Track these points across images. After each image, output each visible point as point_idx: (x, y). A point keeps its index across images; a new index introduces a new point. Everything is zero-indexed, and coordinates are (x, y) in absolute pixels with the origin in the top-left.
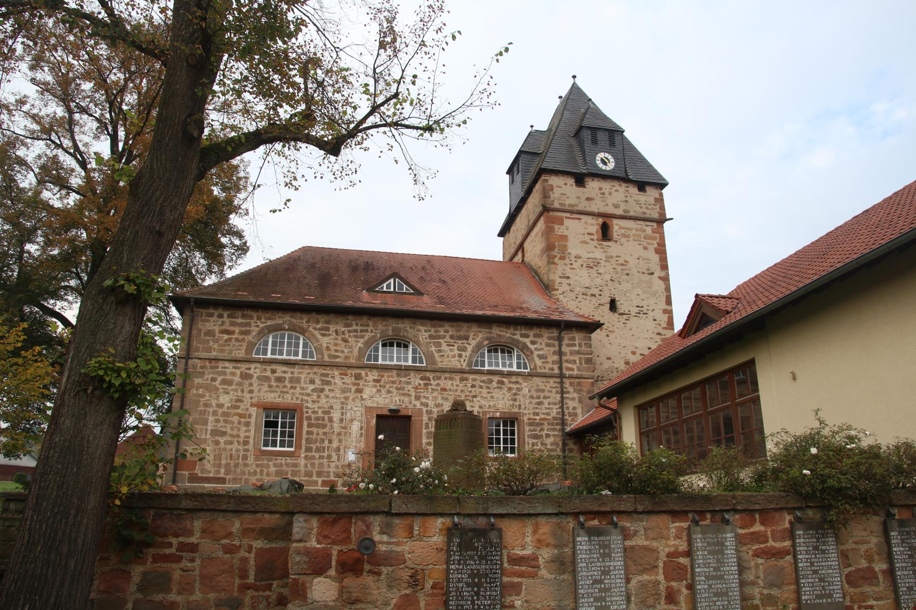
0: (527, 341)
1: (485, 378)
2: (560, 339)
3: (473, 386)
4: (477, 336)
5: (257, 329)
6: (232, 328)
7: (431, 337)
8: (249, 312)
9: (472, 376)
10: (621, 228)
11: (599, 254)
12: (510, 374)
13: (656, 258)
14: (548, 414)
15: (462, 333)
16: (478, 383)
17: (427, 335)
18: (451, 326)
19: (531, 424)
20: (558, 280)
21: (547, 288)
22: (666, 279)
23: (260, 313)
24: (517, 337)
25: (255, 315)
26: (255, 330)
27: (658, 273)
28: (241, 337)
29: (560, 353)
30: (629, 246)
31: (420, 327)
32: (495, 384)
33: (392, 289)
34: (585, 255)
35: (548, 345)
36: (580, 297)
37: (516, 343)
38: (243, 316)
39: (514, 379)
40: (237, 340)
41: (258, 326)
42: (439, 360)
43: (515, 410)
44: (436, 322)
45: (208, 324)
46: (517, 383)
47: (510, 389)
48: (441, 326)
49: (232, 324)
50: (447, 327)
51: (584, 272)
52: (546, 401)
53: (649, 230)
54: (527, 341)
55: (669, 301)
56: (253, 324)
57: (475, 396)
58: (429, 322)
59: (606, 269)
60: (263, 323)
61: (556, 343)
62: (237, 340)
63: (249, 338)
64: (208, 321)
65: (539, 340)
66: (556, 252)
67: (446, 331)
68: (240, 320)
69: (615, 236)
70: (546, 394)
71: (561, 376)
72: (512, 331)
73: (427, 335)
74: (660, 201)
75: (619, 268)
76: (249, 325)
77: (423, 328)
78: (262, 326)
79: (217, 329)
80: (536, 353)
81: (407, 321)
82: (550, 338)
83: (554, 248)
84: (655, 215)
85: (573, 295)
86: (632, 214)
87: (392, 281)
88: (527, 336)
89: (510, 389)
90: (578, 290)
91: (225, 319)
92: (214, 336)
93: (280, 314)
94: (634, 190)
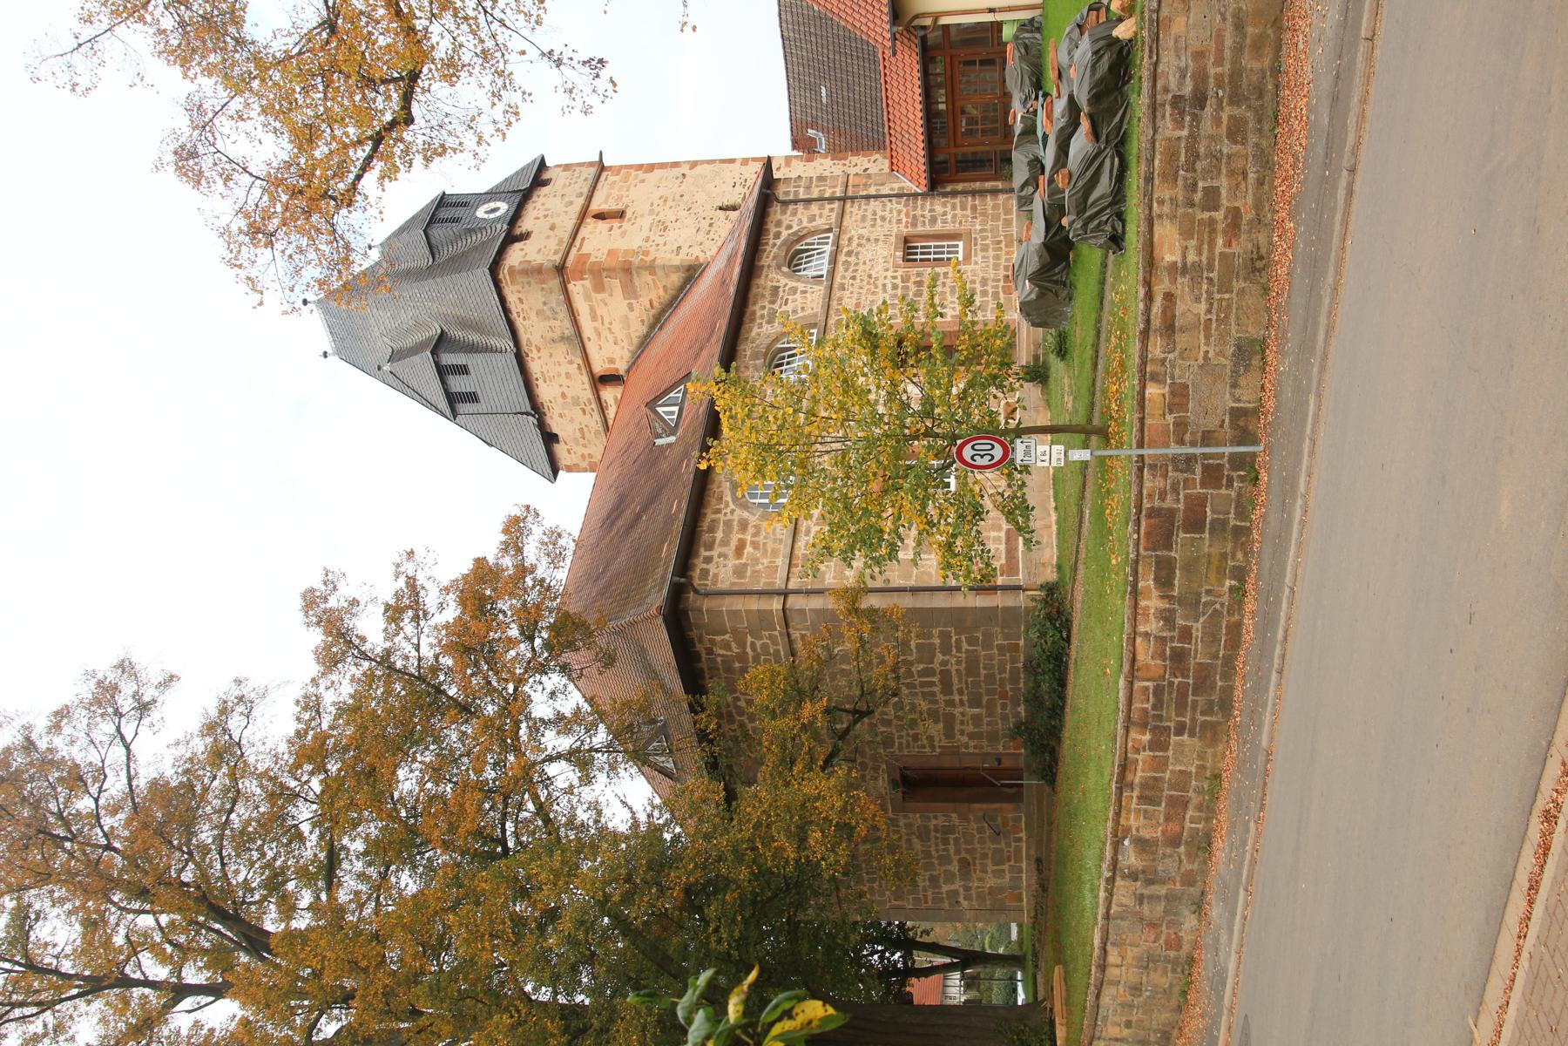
0: (785, 233)
1: (840, 268)
2: (785, 203)
3: (854, 278)
4: (773, 276)
5: (738, 512)
6: (734, 543)
7: (769, 322)
8: (705, 525)
9: (838, 280)
10: (606, 202)
11: (646, 222)
12: (837, 244)
13: (657, 172)
14: (899, 212)
15: (767, 293)
16: (849, 274)
17: (765, 326)
18: (755, 303)
19: (914, 225)
20: (682, 256)
21: (692, 273)
22: (694, 164)
23: (709, 511)
24: (778, 242)
25: (710, 517)
26: (740, 513)
27: (685, 169)
28: (751, 530)
29: (808, 201)
30: (638, 197)
31: (753, 334)
32: (852, 259)
33: (676, 409)
34: (645, 233)
35: (795, 213)
36: (711, 235)
37: (790, 243)
38: (712, 530)
39: (844, 242)
40: (756, 534)
41: (732, 512)
42: (808, 312)
43: (893, 239)
44: (746, 319)
45: (722, 576)
46: (850, 239)
47: (859, 245)
48: (754, 313)
49: (725, 543)
50: (757, 308)
51: (671, 235)
52: (880, 213)
53: (612, 179)
54: (785, 233)
55: (732, 161)
56: (729, 517)
57: (870, 276)
58: (745, 327)
59: (668, 215)
60: (727, 505)
61: (791, 207)
62: (756, 534)
63: (753, 519)
64: (716, 575)
65: (785, 223)
66: (636, 261)
67: (760, 308)
68: (719, 535)
69: (620, 207)
70: (869, 213)
71: (843, 199)
72: (768, 248)
73: (765, 326)
74: (567, 167)
75: (669, 203)
76: (728, 524)
77: (755, 331)
78: (732, 506)
79: (732, 562)
80: (805, 223)
81: (741, 347)
82: (784, 213)
83: (627, 271)
84: (593, 171)
85: (707, 244)
86: (585, 190)
87: (660, 410)
88: (778, 235)
89: (859, 245)
90: (701, 237)
91: (715, 553)
92: (745, 565)
93: (714, 487)
94: (544, 190)
